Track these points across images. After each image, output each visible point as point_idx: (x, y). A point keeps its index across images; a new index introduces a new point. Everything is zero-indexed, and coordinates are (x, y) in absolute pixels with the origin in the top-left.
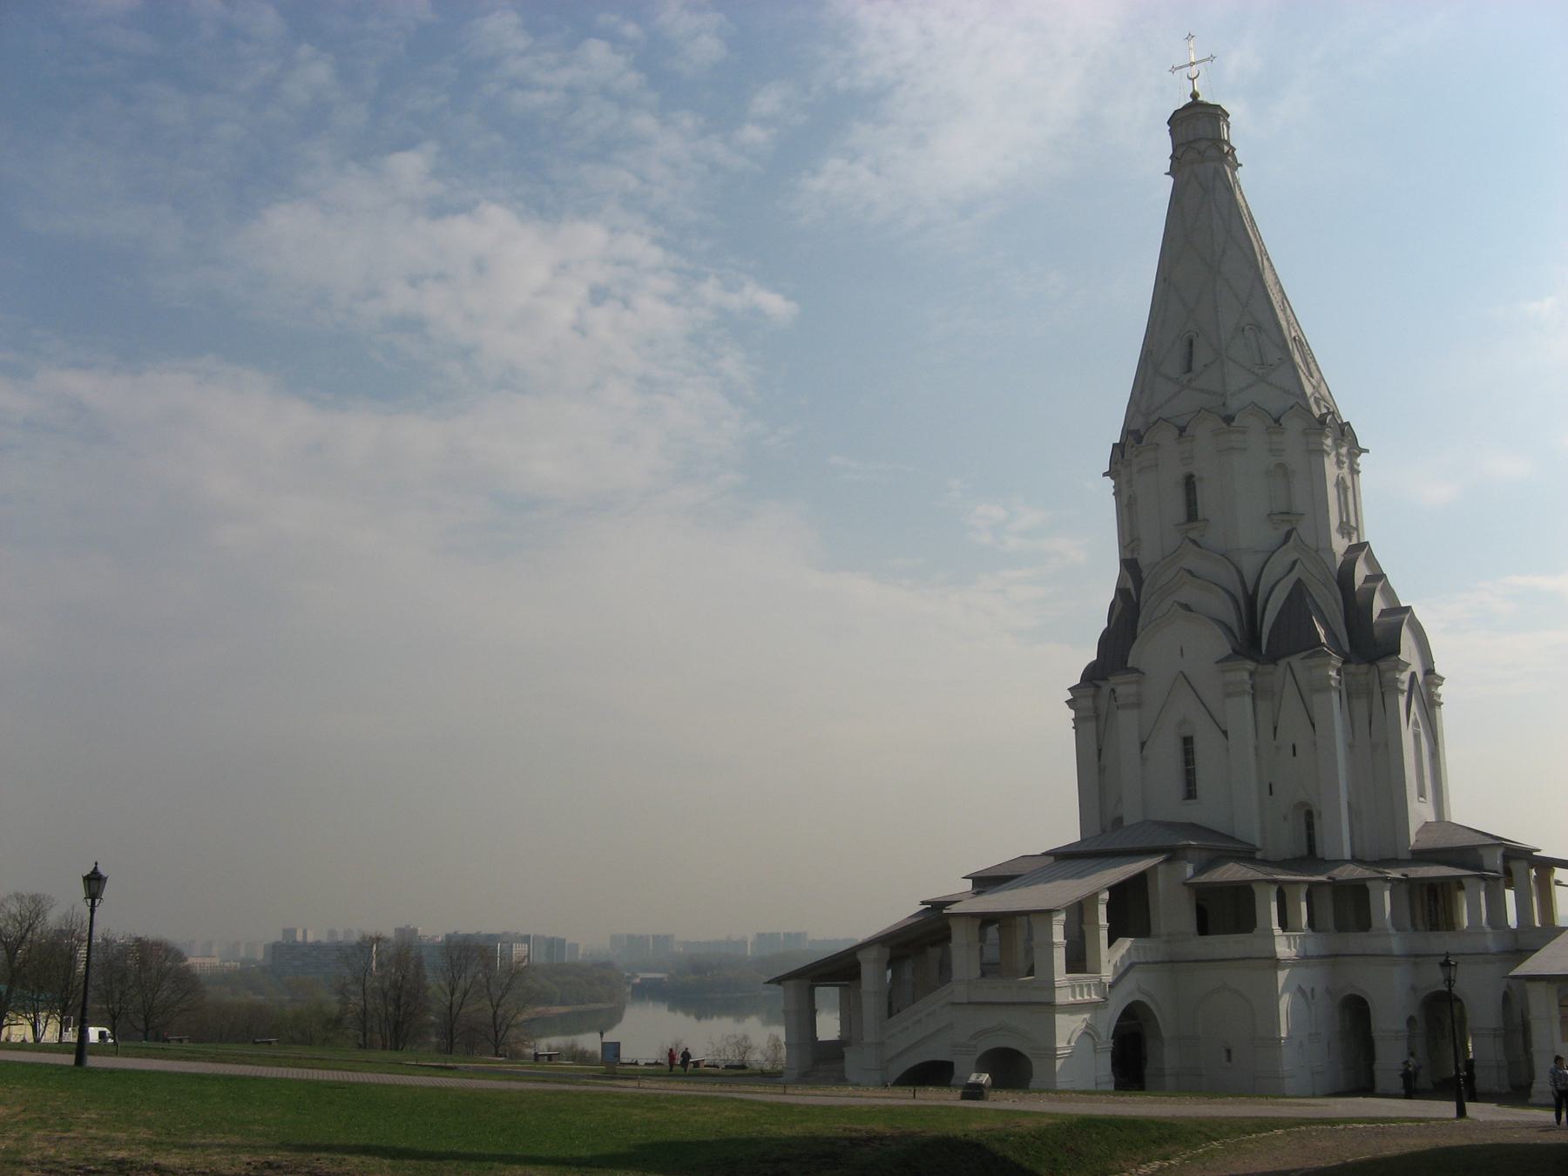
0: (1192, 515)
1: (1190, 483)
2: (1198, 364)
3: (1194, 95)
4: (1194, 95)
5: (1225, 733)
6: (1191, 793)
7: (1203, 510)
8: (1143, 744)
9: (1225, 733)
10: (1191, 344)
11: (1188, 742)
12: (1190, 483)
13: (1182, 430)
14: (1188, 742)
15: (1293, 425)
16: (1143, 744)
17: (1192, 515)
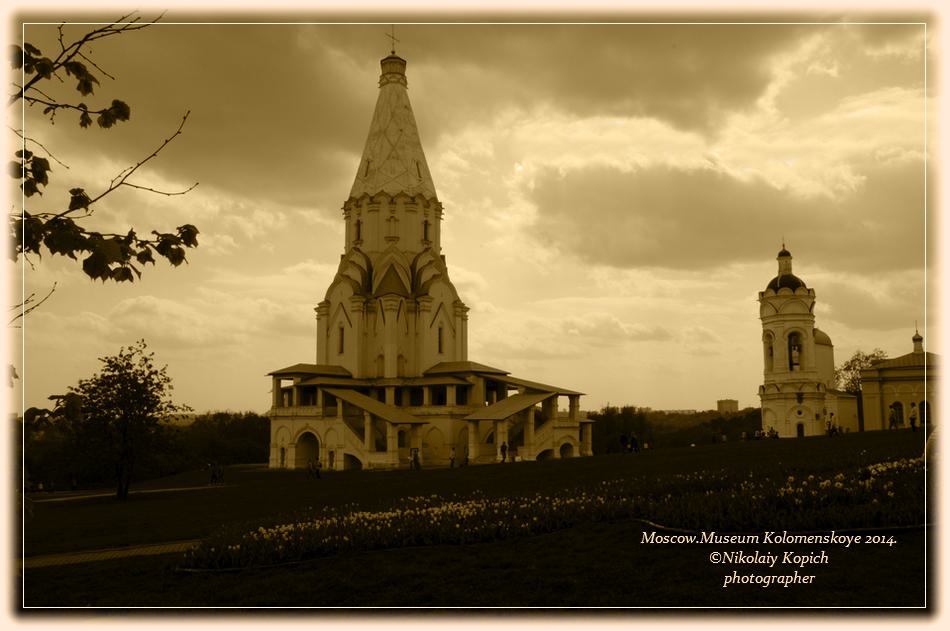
5: (454, 331)
6: (440, 351)
9: (454, 331)
14: (440, 329)
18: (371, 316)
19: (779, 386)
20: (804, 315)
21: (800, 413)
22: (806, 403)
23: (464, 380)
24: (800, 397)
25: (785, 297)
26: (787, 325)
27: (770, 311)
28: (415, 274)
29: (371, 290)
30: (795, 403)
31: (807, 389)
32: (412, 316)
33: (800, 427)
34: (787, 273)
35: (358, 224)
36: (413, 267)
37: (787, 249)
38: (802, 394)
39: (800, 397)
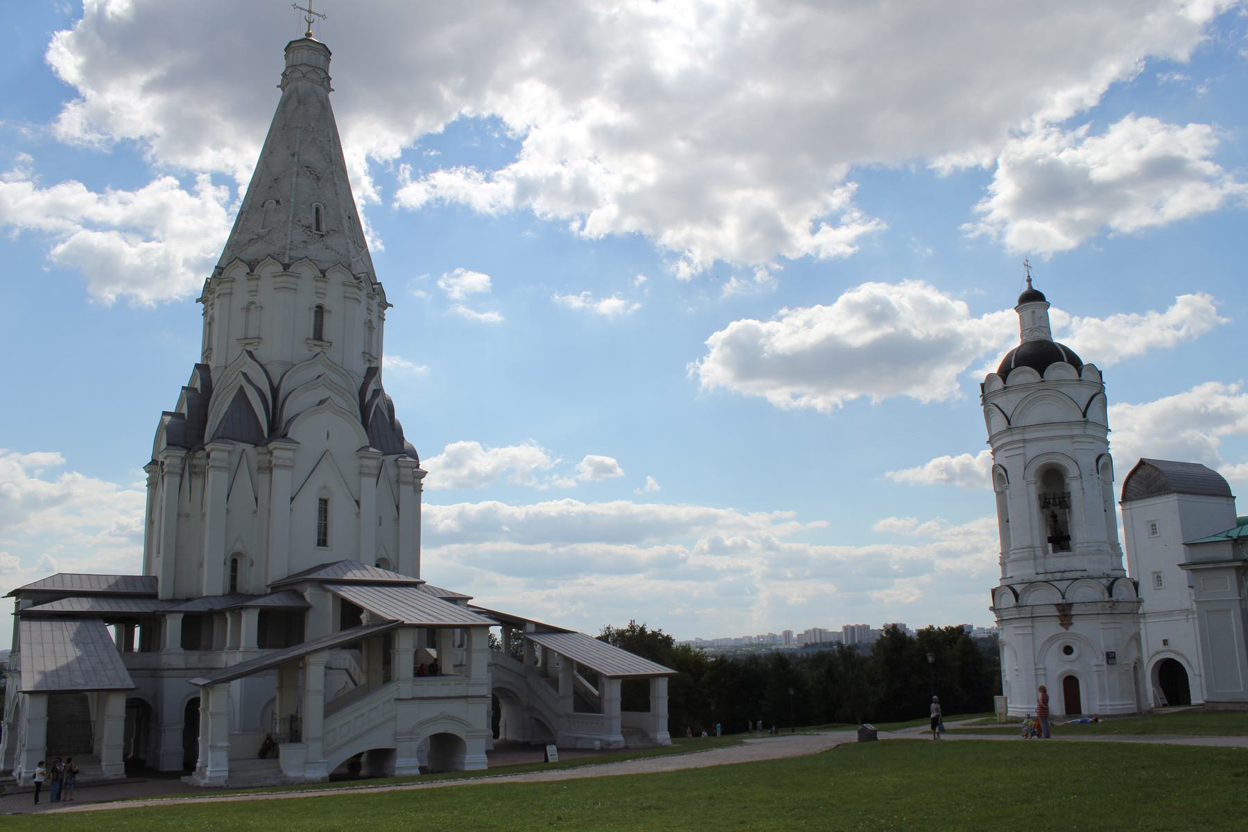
0: (318, 335)
1: (320, 311)
2: (323, 227)
3: (309, 35)
4: (309, 35)
5: (358, 502)
6: (322, 542)
7: (325, 338)
8: (292, 499)
9: (358, 502)
10: (317, 210)
11: (324, 503)
12: (320, 311)
13: (323, 272)
14: (324, 503)
15: (378, 299)
16: (292, 499)
17: (318, 335)
18: (198, 482)
19: (1018, 588)
20: (1069, 423)
21: (1068, 650)
22: (1080, 627)
23: (303, 598)
24: (1065, 613)
25: (1025, 387)
26: (1033, 450)
27: (999, 423)
28: (275, 400)
29: (203, 437)
30: (1054, 627)
31: (1081, 594)
32: (264, 477)
33: (1071, 685)
34: (1039, 336)
35: (210, 324)
36: (275, 391)
37: (1035, 287)
38: (1071, 605)
39: (1065, 613)
